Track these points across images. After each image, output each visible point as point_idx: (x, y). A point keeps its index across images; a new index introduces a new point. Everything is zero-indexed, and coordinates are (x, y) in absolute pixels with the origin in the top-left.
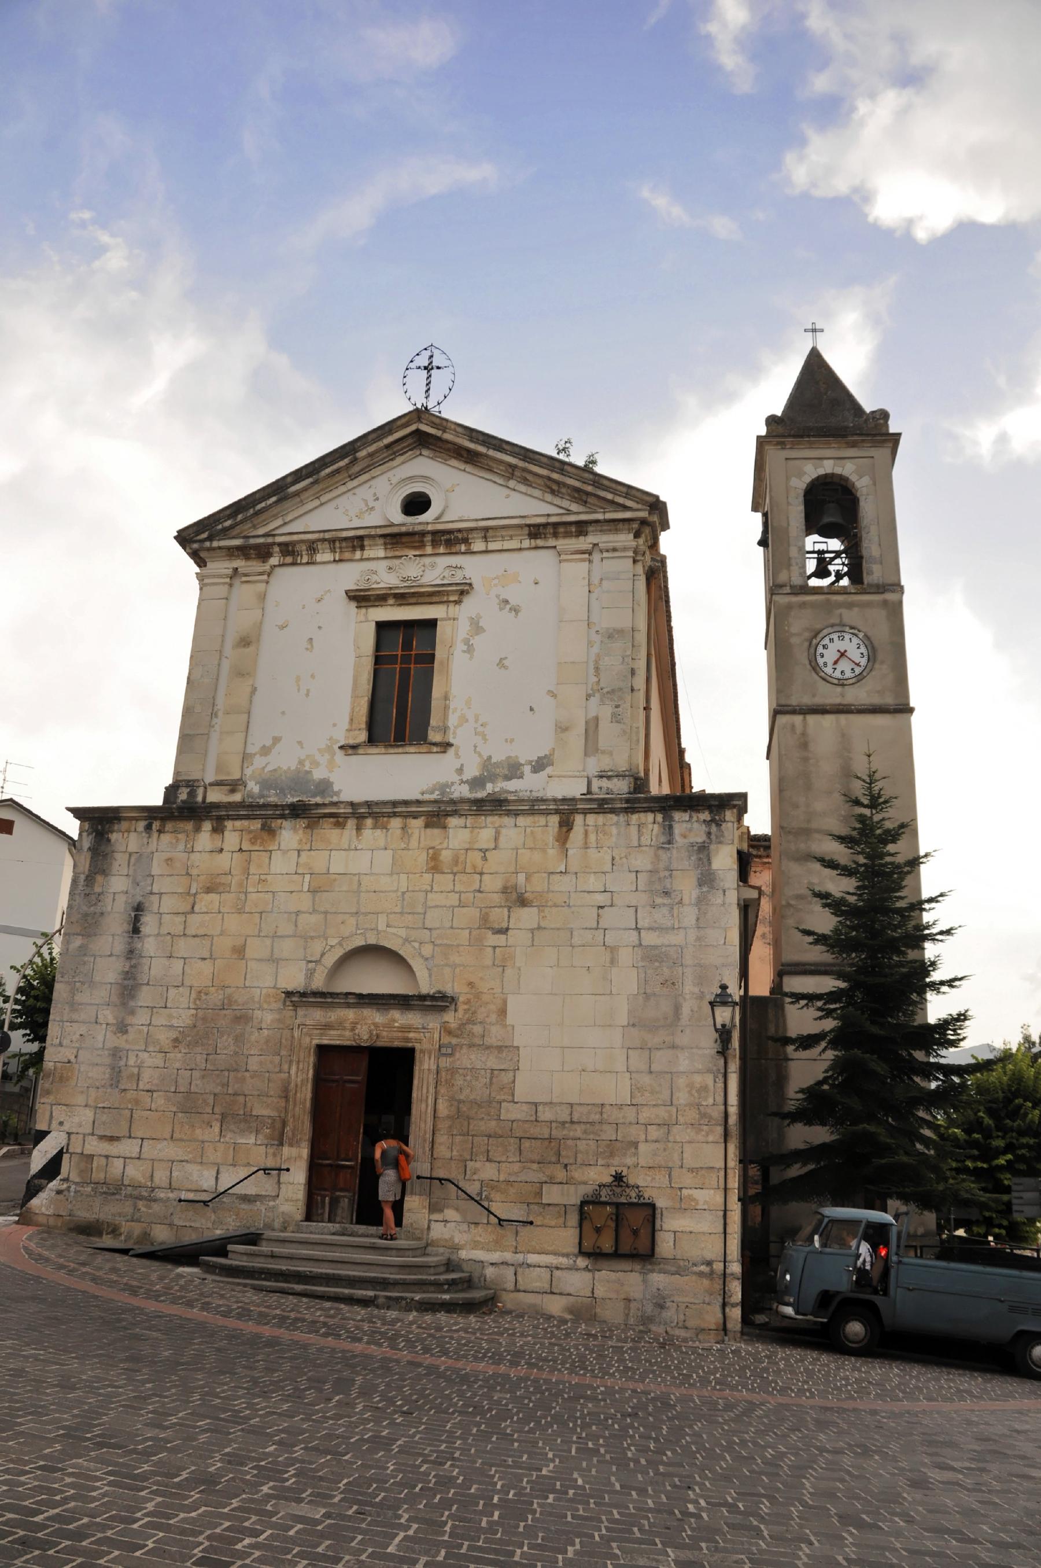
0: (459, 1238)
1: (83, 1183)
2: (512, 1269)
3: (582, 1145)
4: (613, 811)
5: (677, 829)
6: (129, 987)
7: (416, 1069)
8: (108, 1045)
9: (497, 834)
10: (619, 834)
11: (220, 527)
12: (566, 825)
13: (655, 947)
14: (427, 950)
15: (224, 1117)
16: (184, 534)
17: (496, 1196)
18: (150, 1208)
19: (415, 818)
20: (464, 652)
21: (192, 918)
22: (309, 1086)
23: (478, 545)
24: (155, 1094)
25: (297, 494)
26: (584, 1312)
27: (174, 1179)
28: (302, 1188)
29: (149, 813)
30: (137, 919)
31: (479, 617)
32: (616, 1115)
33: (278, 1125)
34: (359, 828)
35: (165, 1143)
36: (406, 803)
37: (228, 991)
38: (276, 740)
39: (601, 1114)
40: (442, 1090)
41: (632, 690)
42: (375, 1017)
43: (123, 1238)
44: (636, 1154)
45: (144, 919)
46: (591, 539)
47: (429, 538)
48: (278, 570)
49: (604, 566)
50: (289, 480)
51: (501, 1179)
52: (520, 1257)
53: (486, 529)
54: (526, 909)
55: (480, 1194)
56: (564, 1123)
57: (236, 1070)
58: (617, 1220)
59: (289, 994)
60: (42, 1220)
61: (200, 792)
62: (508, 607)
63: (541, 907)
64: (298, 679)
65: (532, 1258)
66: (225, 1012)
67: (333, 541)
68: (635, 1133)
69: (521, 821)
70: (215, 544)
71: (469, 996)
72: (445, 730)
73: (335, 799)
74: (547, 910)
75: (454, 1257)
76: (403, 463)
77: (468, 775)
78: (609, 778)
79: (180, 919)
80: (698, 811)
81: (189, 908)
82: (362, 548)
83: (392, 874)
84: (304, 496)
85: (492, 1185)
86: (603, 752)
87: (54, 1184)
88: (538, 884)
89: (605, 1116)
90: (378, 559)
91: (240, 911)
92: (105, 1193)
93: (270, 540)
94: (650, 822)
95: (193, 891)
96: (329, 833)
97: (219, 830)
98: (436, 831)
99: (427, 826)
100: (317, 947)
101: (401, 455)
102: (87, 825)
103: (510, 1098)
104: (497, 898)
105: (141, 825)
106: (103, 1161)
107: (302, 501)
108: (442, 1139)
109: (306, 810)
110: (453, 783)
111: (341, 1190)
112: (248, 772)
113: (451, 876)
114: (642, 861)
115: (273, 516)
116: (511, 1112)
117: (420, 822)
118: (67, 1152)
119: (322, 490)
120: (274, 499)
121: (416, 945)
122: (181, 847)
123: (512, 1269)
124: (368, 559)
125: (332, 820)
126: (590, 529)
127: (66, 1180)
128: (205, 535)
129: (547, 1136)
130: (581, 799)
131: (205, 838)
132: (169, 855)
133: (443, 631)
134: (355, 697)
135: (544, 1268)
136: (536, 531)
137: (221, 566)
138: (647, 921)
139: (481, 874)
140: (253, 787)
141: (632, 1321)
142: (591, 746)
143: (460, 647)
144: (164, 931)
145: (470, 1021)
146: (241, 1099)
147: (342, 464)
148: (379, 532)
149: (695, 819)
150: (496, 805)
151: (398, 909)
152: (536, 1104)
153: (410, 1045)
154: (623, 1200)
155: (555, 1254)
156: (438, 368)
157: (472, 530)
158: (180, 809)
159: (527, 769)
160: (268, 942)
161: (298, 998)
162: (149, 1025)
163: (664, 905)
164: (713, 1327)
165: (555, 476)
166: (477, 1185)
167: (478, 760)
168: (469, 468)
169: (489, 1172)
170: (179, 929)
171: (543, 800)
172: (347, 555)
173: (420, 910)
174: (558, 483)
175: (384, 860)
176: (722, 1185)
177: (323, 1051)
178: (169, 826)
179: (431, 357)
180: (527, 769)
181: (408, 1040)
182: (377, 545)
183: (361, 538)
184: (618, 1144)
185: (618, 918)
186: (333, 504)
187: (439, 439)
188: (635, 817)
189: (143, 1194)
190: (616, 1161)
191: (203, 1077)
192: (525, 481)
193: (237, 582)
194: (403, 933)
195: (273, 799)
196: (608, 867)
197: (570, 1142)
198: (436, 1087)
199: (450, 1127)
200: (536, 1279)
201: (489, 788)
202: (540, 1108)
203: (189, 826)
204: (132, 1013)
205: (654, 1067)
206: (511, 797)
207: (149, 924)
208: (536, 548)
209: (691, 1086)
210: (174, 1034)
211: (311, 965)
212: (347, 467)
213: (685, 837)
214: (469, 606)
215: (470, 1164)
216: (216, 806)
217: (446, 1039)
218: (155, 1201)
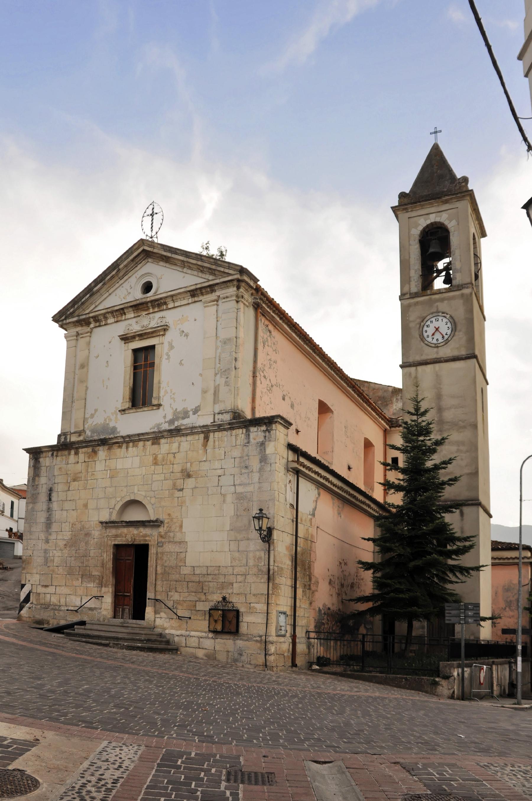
2: (184, 638)
3: (211, 584)
4: (225, 430)
6: (49, 523)
7: (149, 553)
8: (43, 548)
9: (180, 444)
10: (227, 440)
11: (69, 313)
12: (207, 438)
13: (242, 493)
14: (153, 500)
16: (55, 318)
17: (180, 607)
18: (59, 614)
19: (148, 441)
20: (166, 359)
22: (111, 562)
23: (171, 305)
24: (59, 568)
25: (98, 291)
26: (211, 657)
28: (110, 604)
29: (52, 448)
30: (50, 495)
32: (223, 571)
33: (101, 579)
34: (127, 448)
35: (63, 587)
37: (82, 523)
38: (96, 410)
39: (219, 570)
40: (159, 562)
41: (235, 369)
42: (134, 531)
45: (53, 495)
46: (218, 293)
47: (150, 304)
48: (95, 330)
50: (93, 285)
51: (181, 599)
52: (188, 633)
53: (172, 296)
54: (190, 479)
55: (173, 606)
56: (204, 575)
57: (86, 556)
58: (223, 617)
59: (102, 523)
61: (68, 437)
62: (184, 334)
63: (196, 478)
64: (103, 381)
65: (193, 633)
67: (112, 312)
68: (232, 579)
69: (189, 438)
70: (68, 321)
71: (169, 520)
72: (159, 398)
73: (118, 435)
74: (198, 479)
75: (163, 633)
76: (141, 268)
77: (167, 420)
78: (222, 413)
79: (65, 493)
81: (67, 489)
82: (125, 314)
83: (139, 468)
84: (101, 291)
85: (178, 602)
86: (221, 402)
88: (195, 468)
89: (220, 571)
90: (132, 318)
95: (69, 481)
97: (77, 453)
98: (156, 446)
99: (153, 444)
100: (113, 502)
101: (140, 263)
102: (31, 456)
103: (184, 564)
104: (179, 475)
107: (101, 294)
108: (159, 582)
110: (162, 423)
112: (86, 426)
113: (161, 466)
114: (236, 453)
115: (91, 304)
116: (185, 571)
117: (149, 443)
119: (109, 287)
120: (88, 295)
121: (149, 498)
122: (64, 462)
123: (184, 638)
124: (128, 319)
125: (117, 445)
127: (32, 603)
128: (63, 318)
129: (198, 581)
130: (210, 425)
131: (72, 458)
132: (59, 466)
133: (158, 349)
134: (124, 386)
135: (195, 637)
136: (195, 293)
137: (73, 331)
138: (238, 481)
139: (173, 464)
140: (88, 433)
141: (229, 661)
143: (165, 357)
144: (60, 499)
145: (169, 531)
146: (88, 568)
147: (114, 273)
148: (129, 305)
149: (259, 430)
150: (176, 432)
151: (142, 483)
152: (194, 567)
153: (147, 543)
155: (201, 632)
156: (156, 213)
157: (167, 297)
158: (62, 445)
159: (191, 413)
160: (96, 501)
161: (107, 524)
163: (246, 473)
164: (261, 664)
166: (172, 602)
167: (172, 411)
168: (167, 265)
169: (176, 597)
170: (64, 498)
171: (196, 427)
172: (119, 318)
174: (202, 266)
175: (137, 460)
176: (266, 602)
177: (117, 547)
178: (60, 453)
179: (153, 208)
180: (191, 413)
181: (146, 540)
182: (130, 311)
183: (122, 309)
184: (225, 584)
185: (227, 480)
186: (114, 293)
188: (234, 432)
189: (56, 608)
190: (224, 591)
191: (75, 560)
192: (190, 268)
193: (79, 338)
194: (143, 493)
195: (96, 438)
196: (223, 457)
197: (206, 583)
198: (156, 561)
199: (162, 578)
200: (193, 642)
201: (176, 424)
202: (195, 569)
203: (66, 453)
204: (50, 534)
205: (240, 549)
206: (182, 428)
208: (195, 302)
209: (254, 557)
210: (64, 543)
211: (111, 510)
212: (117, 273)
214: (169, 335)
215: (169, 593)
216: (74, 443)
217: (160, 540)
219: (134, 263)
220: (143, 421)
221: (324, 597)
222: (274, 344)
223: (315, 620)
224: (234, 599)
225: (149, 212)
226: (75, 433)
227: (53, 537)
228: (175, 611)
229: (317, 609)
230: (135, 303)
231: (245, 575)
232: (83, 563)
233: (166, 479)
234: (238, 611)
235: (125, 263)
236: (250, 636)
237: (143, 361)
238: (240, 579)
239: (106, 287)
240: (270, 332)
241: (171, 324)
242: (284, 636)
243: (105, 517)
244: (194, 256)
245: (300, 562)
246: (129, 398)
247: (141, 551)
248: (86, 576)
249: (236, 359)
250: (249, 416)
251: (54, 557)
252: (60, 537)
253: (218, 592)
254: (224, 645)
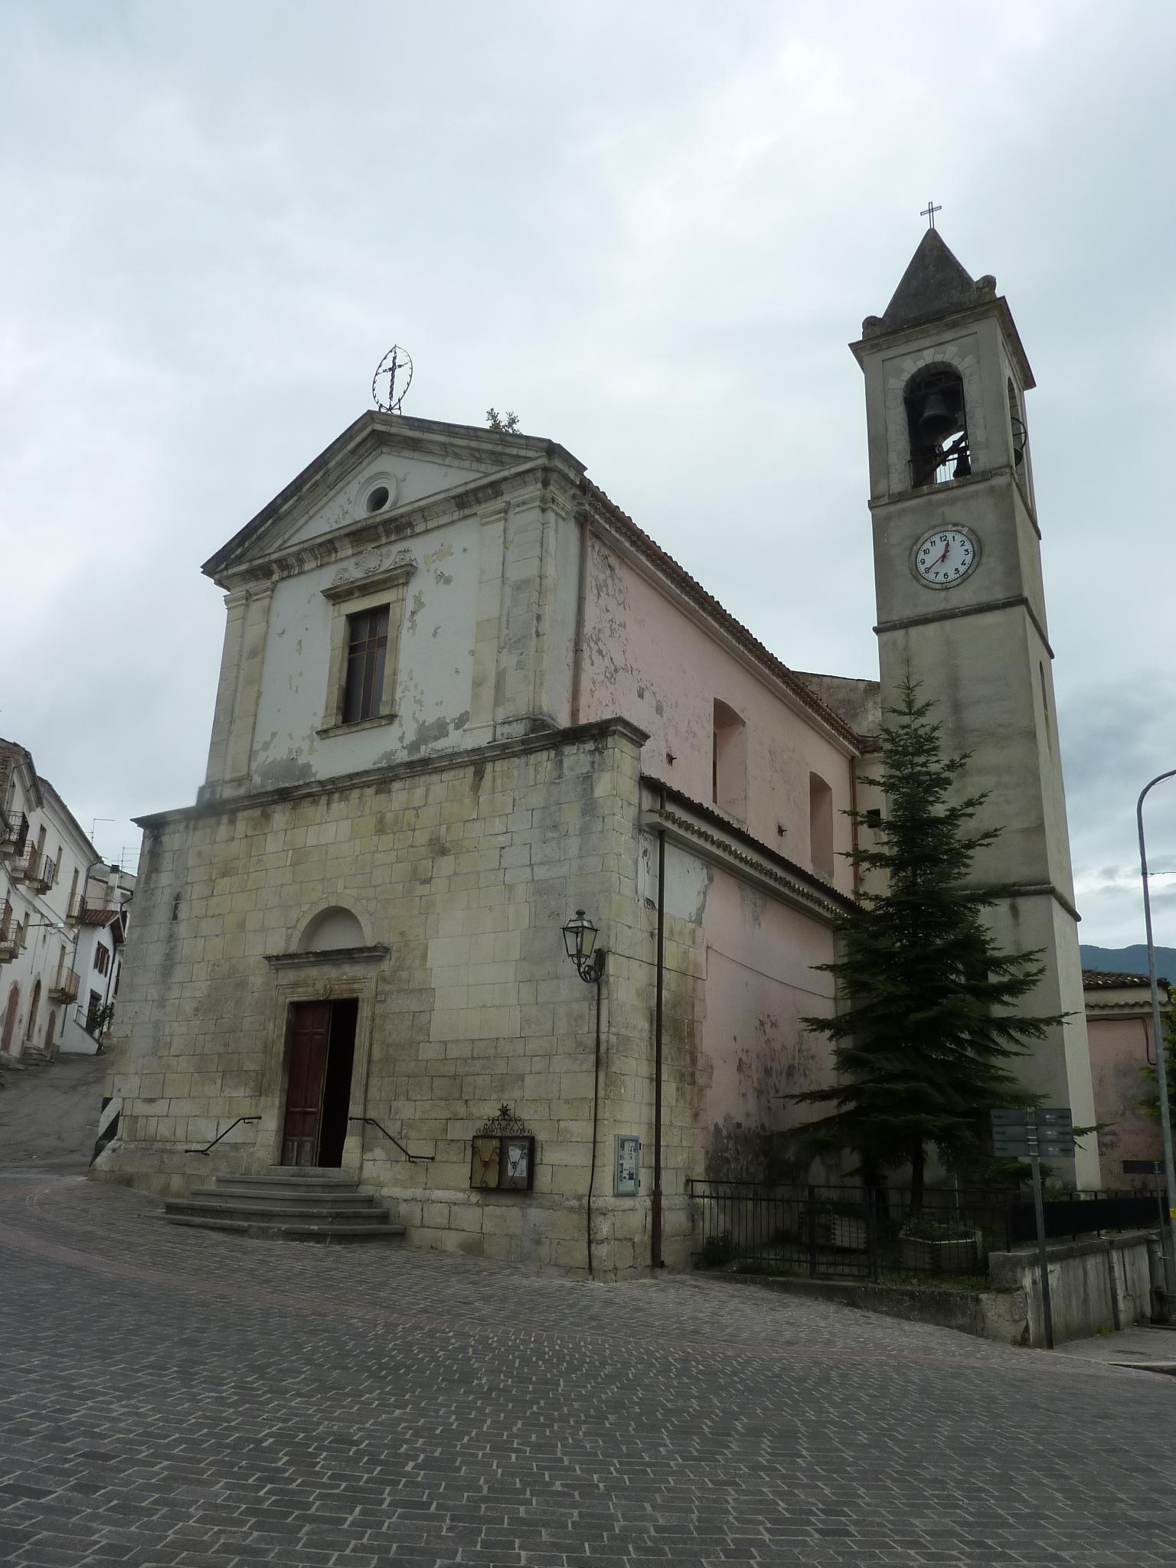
0: (385, 1176)
4: (515, 755)
5: (567, 762)
9: (428, 790)
12: (479, 775)
17: (413, 1134)
21: (214, 901)
23: (419, 529)
25: (288, 513)
29: (187, 816)
30: (176, 907)
31: (421, 593)
34: (328, 804)
36: (358, 774)
38: (274, 735)
40: (376, 1035)
42: (331, 972)
44: (522, 1087)
46: (506, 498)
47: (381, 529)
49: (517, 520)
50: (279, 501)
53: (422, 510)
56: (466, 1059)
59: (268, 958)
65: (439, 1194)
67: (311, 549)
69: (446, 776)
70: (230, 572)
72: (392, 702)
77: (407, 742)
78: (509, 723)
80: (584, 742)
91: (244, 891)
94: (544, 760)
96: (308, 810)
97: (232, 821)
98: (383, 796)
99: (377, 793)
105: (182, 827)
106: (144, 1120)
108: (374, 1081)
109: (292, 794)
111: (308, 1135)
114: (536, 799)
116: (429, 1052)
124: (342, 559)
126: (504, 487)
136: (464, 501)
140: (257, 779)
142: (499, 697)
143: (407, 624)
147: (317, 477)
148: (342, 532)
150: (420, 768)
152: (445, 1043)
154: (508, 1133)
157: (413, 512)
159: (451, 726)
161: (278, 961)
165: (474, 444)
168: (416, 455)
172: (326, 560)
173: (368, 870)
175: (346, 825)
177: (298, 1009)
180: (451, 726)
181: (353, 991)
183: (331, 541)
187: (389, 434)
188: (533, 757)
192: (457, 456)
195: (270, 788)
196: (509, 809)
197: (470, 1079)
198: (371, 1033)
200: (436, 1215)
203: (212, 821)
204: (169, 989)
205: (540, 999)
207: (183, 906)
208: (465, 517)
210: (194, 1005)
213: (572, 769)
215: (394, 1104)
220: (363, 750)
221: (727, 1099)
222: (620, 591)
223: (707, 1152)
224: (524, 1113)
226: (231, 781)
227: (175, 993)
228: (403, 1143)
229: (712, 1128)
230: (353, 528)
231: (549, 1056)
232: (227, 1045)
233: (399, 861)
234: (532, 1140)
235: (339, 458)
236: (556, 1197)
237: (366, 639)
238: (539, 1064)
239: (303, 504)
240: (612, 569)
241: (421, 565)
242: (633, 1195)
243: (276, 947)
244: (462, 431)
245: (669, 1025)
246: (338, 708)
247: (342, 1013)
248: (231, 1073)
249: (539, 618)
250: (564, 722)
252: (186, 994)
253: (494, 1096)
254: (502, 1219)
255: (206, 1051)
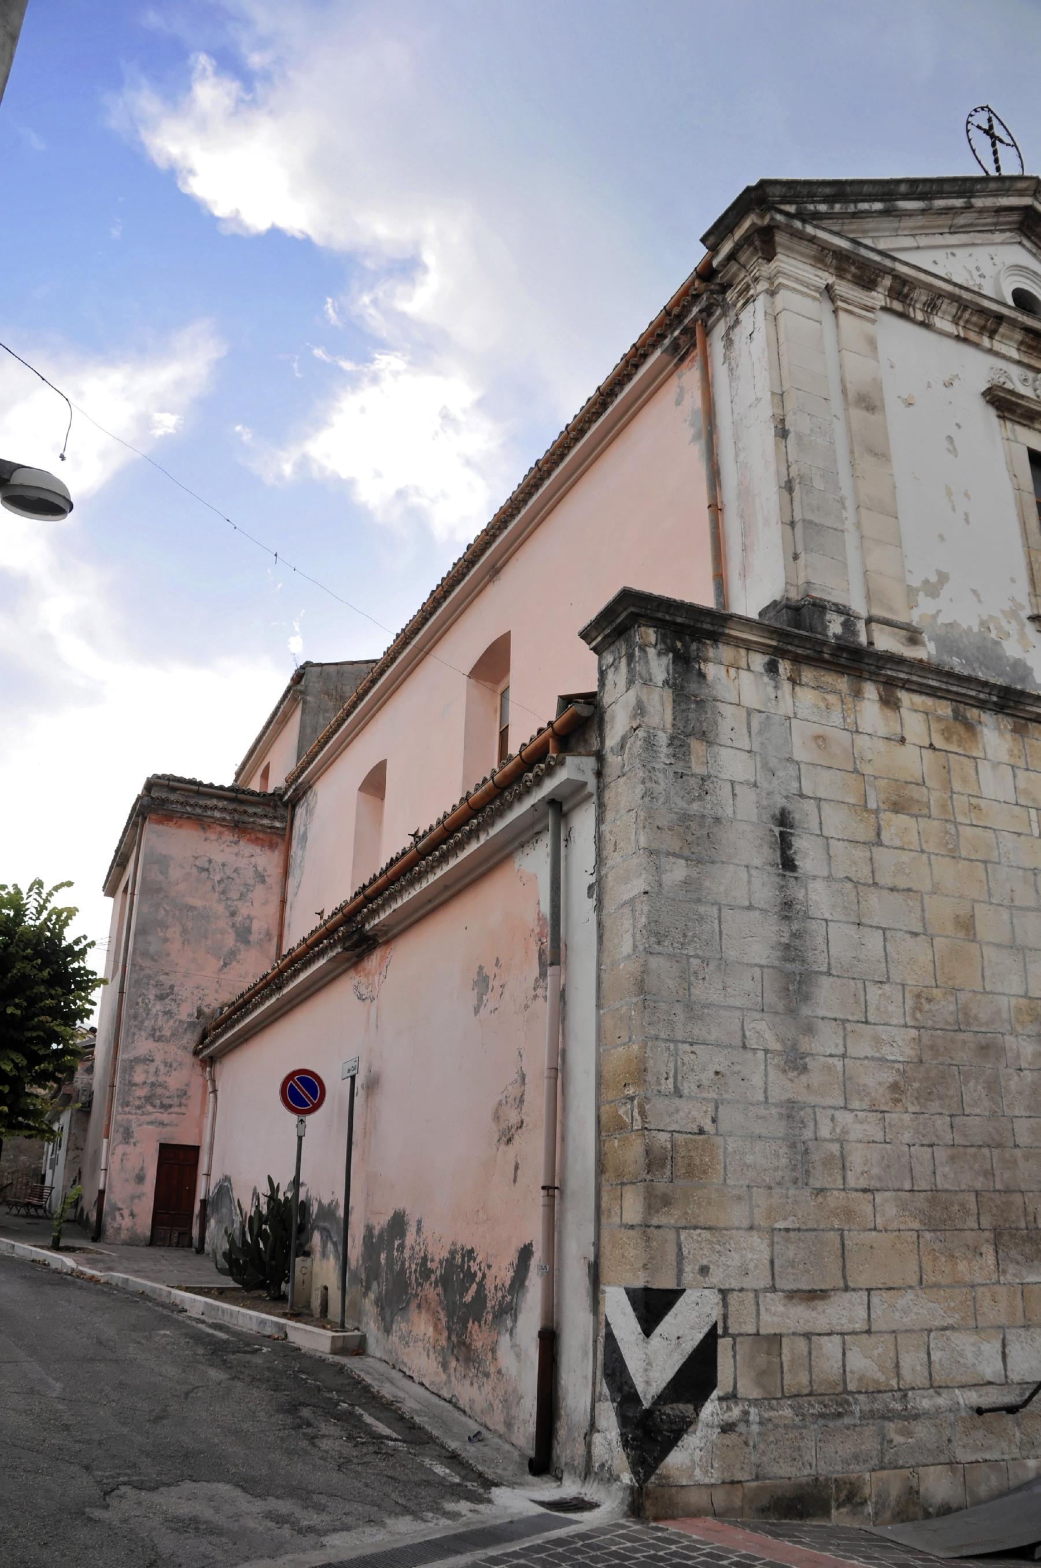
1: (766, 1401)
6: (795, 976)
15: (998, 1234)
18: (909, 1434)
24: (879, 1197)
27: (936, 1367)
30: (784, 843)
37: (963, 997)
43: (870, 1509)
50: (903, 188)
57: (1000, 1146)
60: (696, 1499)
66: (961, 1036)
67: (963, 305)
70: (810, 230)
82: (992, 335)
84: (908, 222)
87: (710, 1409)
92: (822, 1415)
93: (888, 263)
95: (872, 805)
106: (802, 1344)
118: (726, 1334)
119: (922, 227)
120: (878, 206)
127: (731, 1397)
132: (817, 729)
162: (844, 1056)
178: (808, 675)
182: (1011, 339)
191: (952, 1159)
203: (842, 683)
204: (809, 1030)
210: (889, 1077)
218: (916, 1417)
219: (995, 220)
225: (998, 131)
227: (826, 1042)
239: (920, 221)
251: (842, 1142)
252: (861, 1048)
255: (941, 1183)
